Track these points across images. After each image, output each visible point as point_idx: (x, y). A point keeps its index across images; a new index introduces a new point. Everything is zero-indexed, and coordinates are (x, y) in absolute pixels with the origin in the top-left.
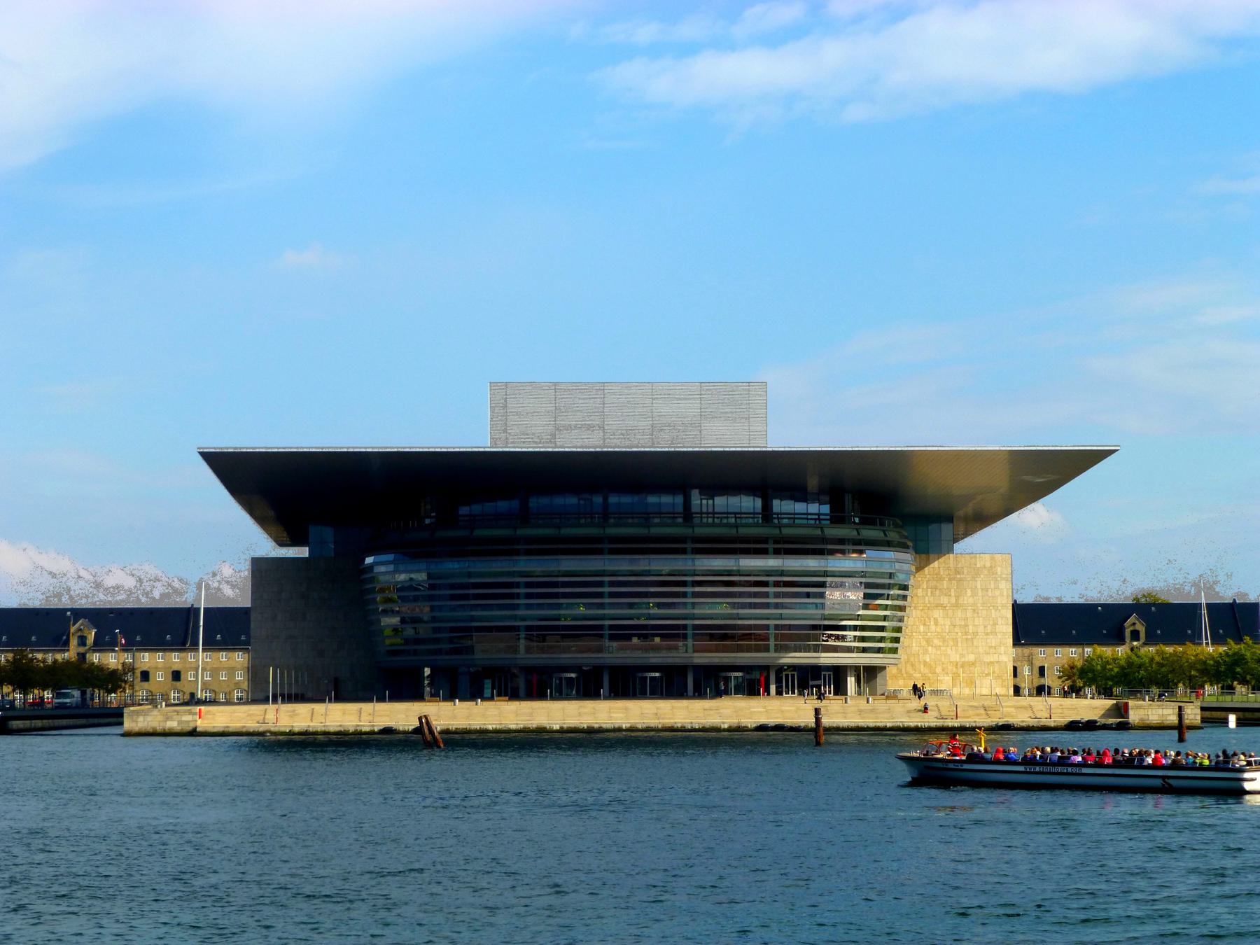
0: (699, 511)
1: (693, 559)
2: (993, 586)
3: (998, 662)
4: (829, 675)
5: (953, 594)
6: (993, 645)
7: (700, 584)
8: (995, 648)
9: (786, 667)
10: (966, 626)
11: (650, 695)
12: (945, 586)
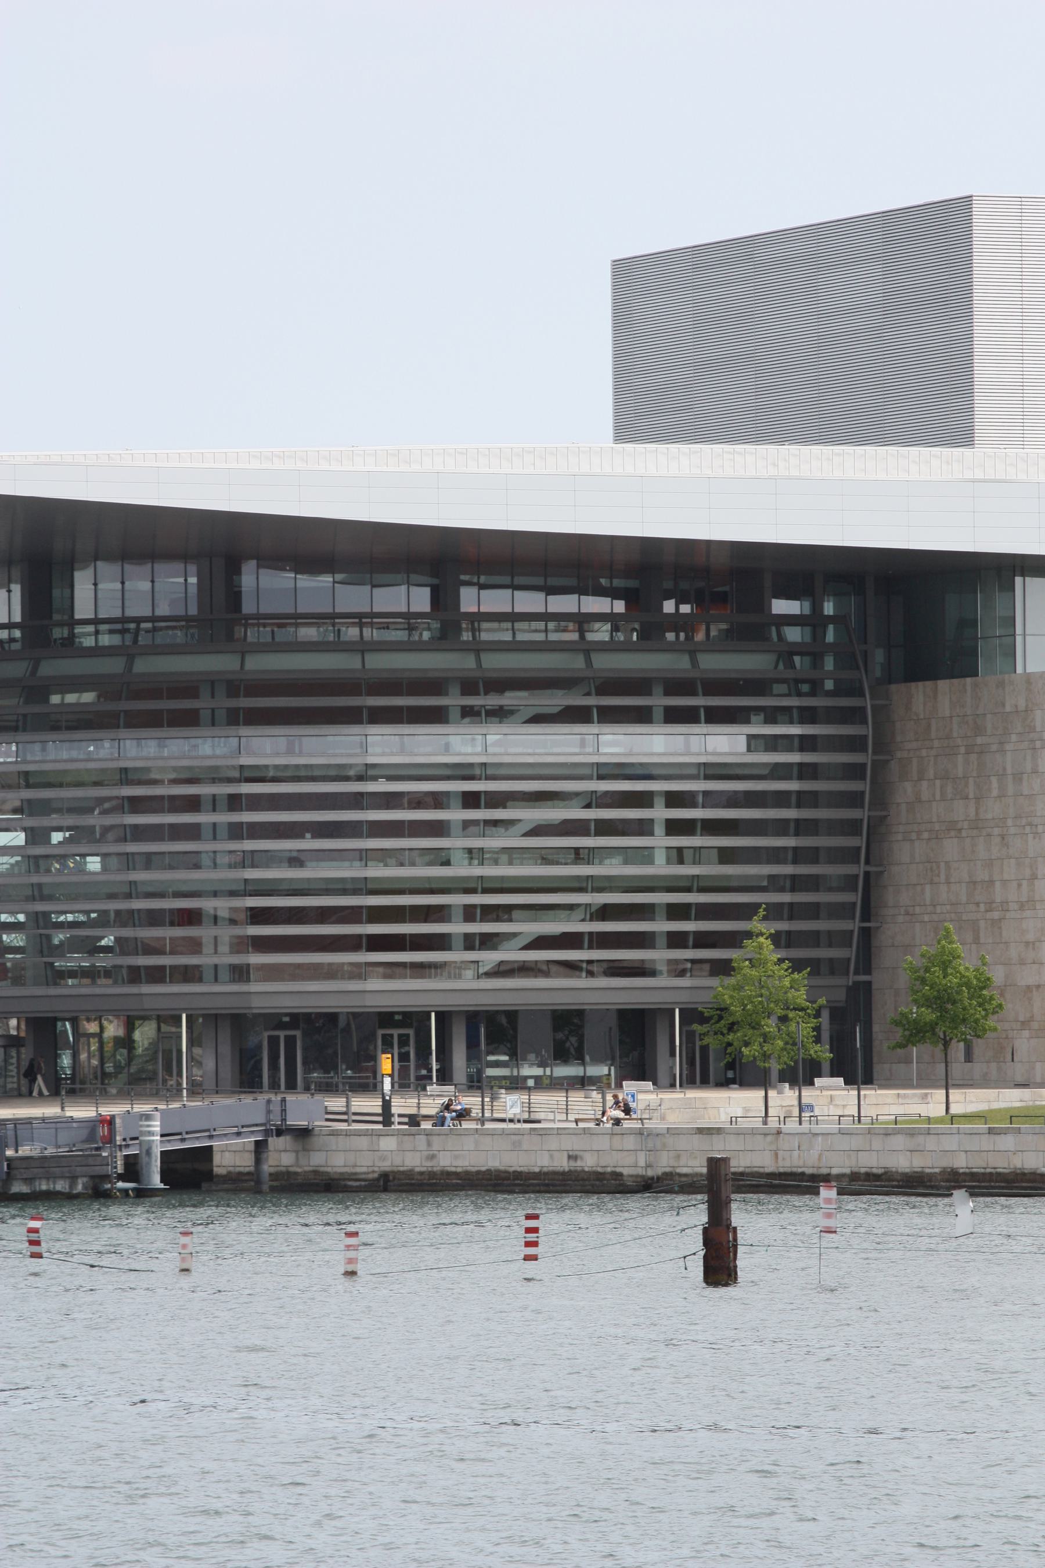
0: (117, 613)
1: (44, 742)
2: (1029, 767)
3: (1038, 987)
4: (290, 1042)
5: (971, 796)
6: (1030, 937)
7: (390, 800)
8: (1033, 943)
9: (286, 1019)
10: (992, 882)
11: (286, 1089)
12: (960, 775)
